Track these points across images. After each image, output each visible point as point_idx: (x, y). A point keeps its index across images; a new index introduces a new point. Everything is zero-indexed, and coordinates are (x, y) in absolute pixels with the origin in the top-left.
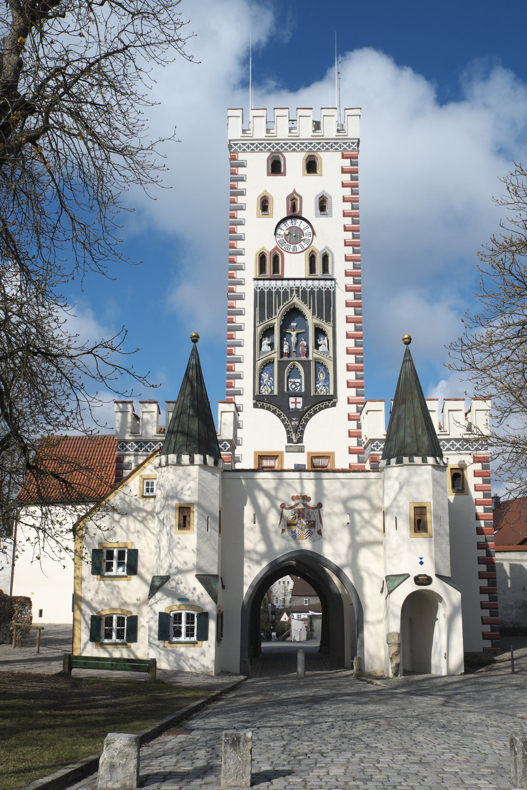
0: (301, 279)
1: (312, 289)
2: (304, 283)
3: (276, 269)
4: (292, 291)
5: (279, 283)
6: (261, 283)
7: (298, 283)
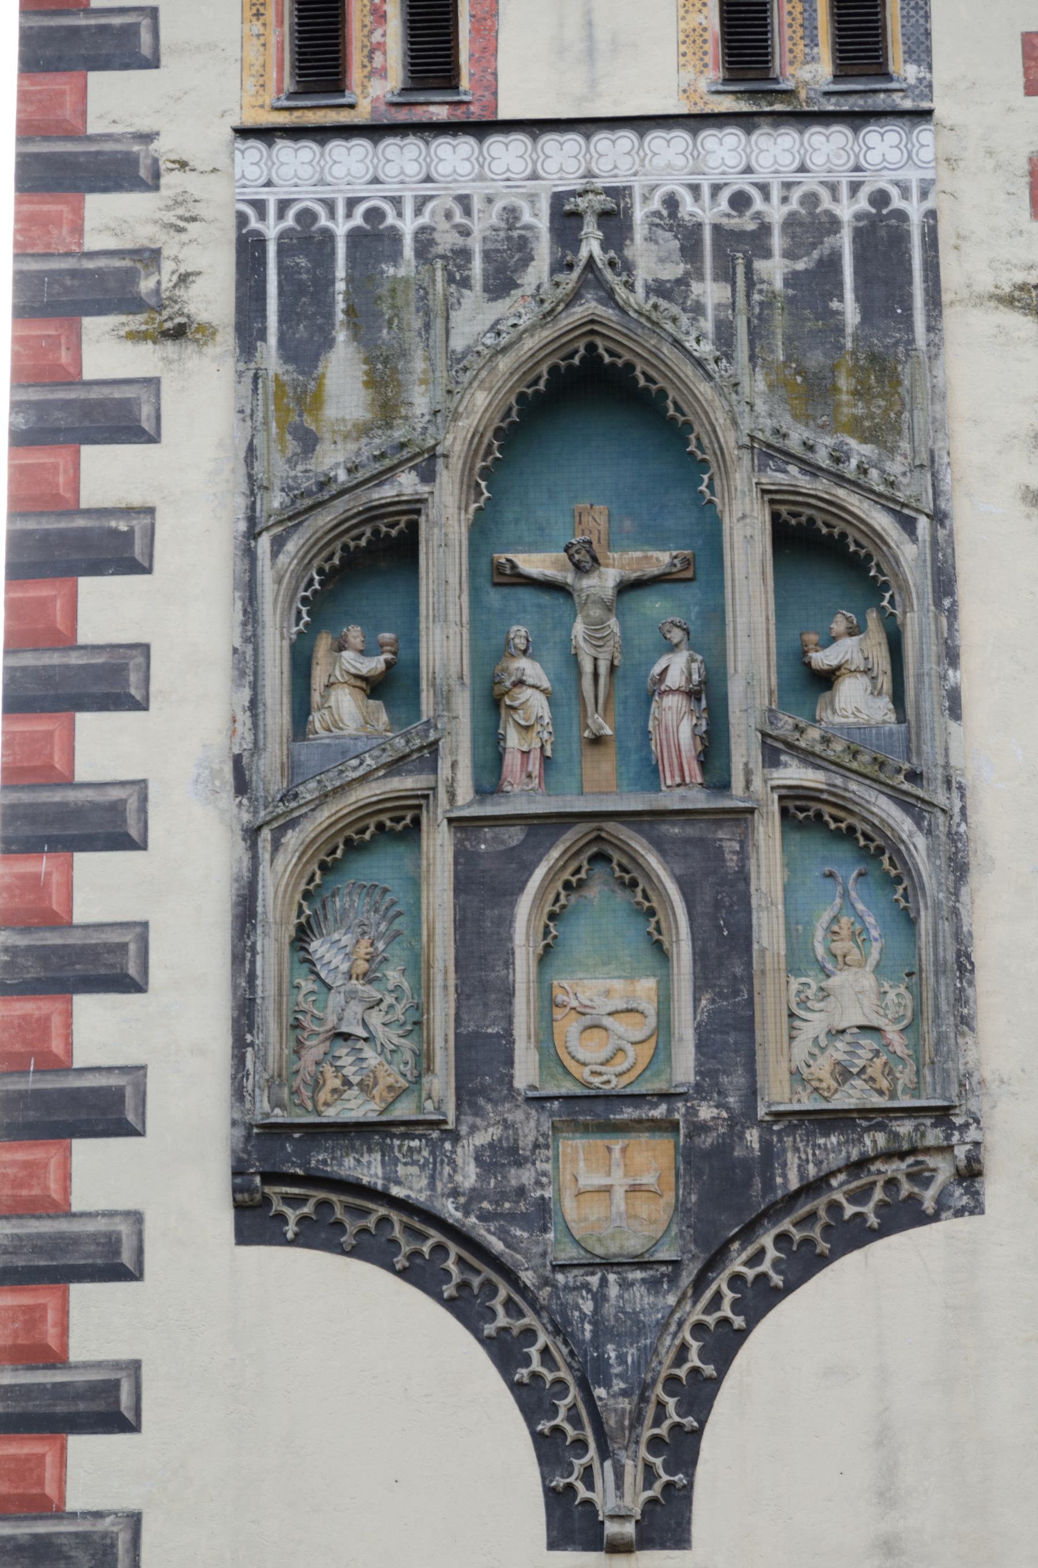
0: (641, 123)
1: (740, 201)
2: (669, 148)
3: (433, 59)
4: (566, 220)
5: (454, 155)
6: (295, 159)
7: (614, 157)
